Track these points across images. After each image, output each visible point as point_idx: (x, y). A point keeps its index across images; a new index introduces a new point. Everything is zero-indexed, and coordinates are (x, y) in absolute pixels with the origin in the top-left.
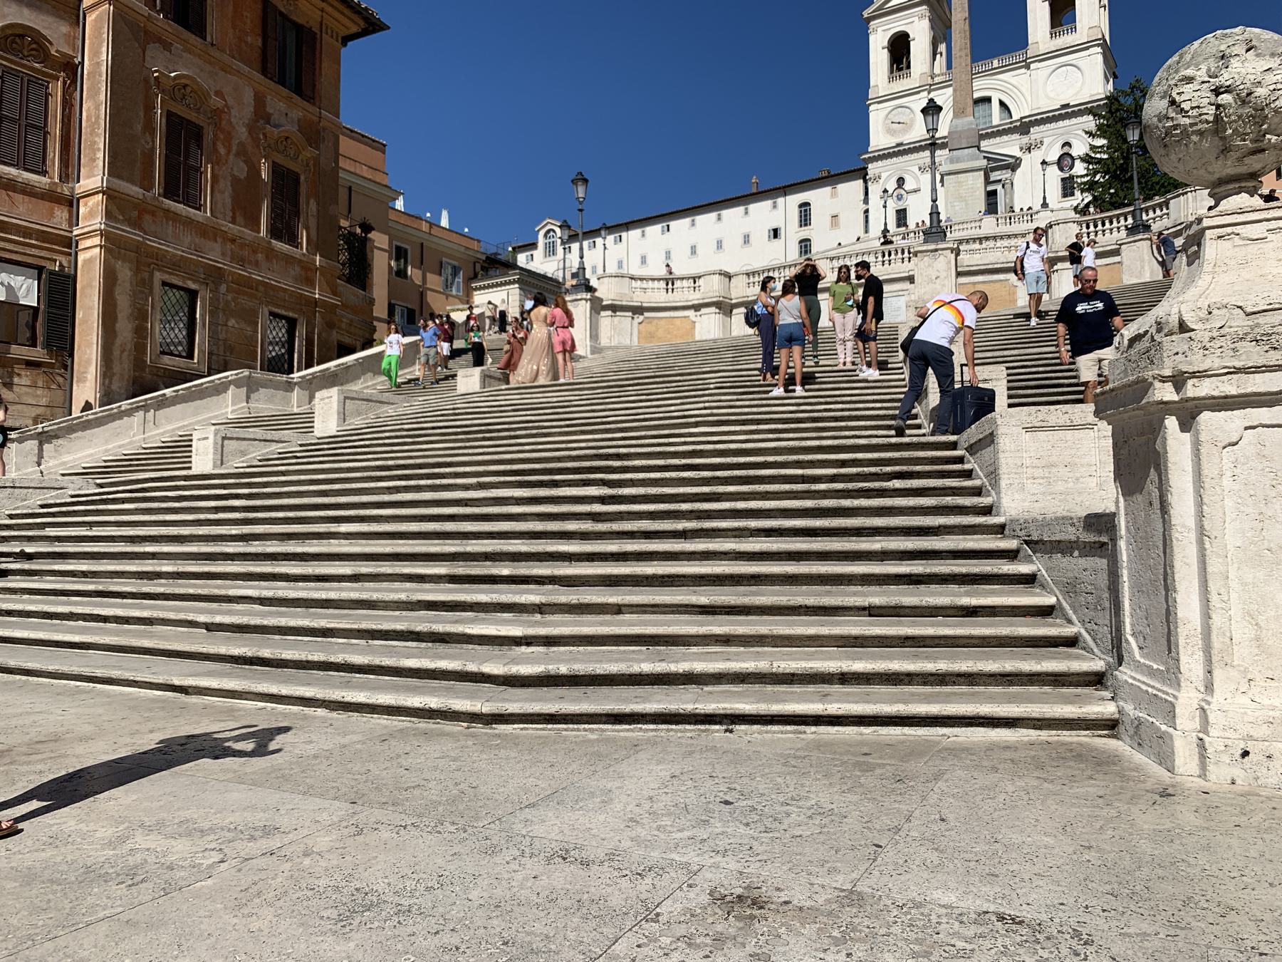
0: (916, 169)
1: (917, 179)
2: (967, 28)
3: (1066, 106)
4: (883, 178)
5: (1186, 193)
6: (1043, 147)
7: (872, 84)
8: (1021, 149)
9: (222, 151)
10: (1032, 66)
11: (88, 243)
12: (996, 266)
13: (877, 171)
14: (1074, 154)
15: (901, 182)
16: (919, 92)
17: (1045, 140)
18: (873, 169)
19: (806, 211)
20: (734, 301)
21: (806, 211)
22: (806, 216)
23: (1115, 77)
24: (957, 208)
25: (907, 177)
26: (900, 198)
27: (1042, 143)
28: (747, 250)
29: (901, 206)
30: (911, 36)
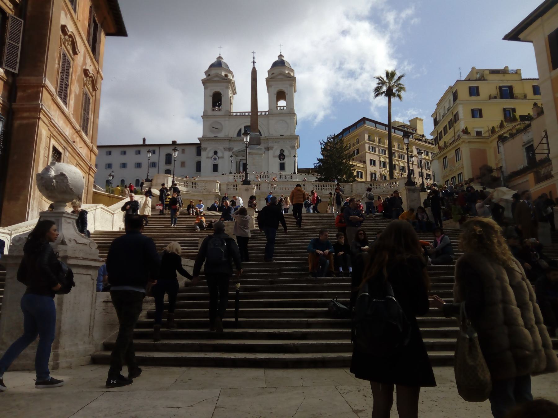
3: (283, 135)
4: (209, 149)
6: (274, 149)
9: (74, 77)
11: (26, 115)
15: (216, 153)
26: (215, 159)
29: (215, 162)
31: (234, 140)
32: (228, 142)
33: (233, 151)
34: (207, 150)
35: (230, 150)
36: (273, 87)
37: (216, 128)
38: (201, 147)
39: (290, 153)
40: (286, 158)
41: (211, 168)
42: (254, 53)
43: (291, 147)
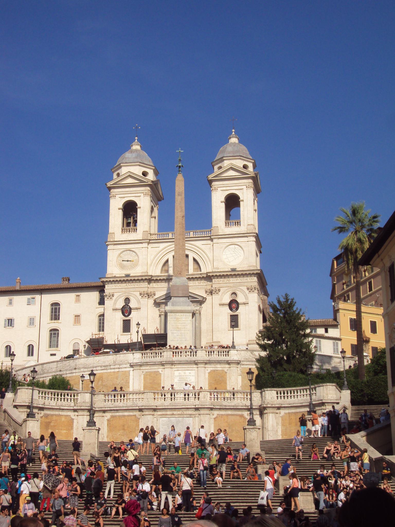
0: (138, 294)
1: (139, 302)
2: (184, 222)
4: (116, 295)
5: (323, 386)
6: (220, 293)
7: (111, 231)
8: (206, 292)
10: (215, 241)
12: (238, 407)
13: (111, 291)
14: (239, 301)
15: (127, 300)
16: (141, 243)
17: (221, 289)
18: (109, 289)
19: (56, 309)
20: (97, 409)
21: (56, 309)
22: (56, 312)
23: (260, 252)
24: (175, 334)
25: (132, 299)
27: (219, 290)
28: (9, 329)
30: (139, 205)
31: (157, 280)
32: (147, 283)
33: (156, 297)
34: (114, 298)
35: (149, 295)
36: (219, 189)
37: (128, 261)
38: (104, 291)
39: (246, 298)
40: (240, 307)
41: (119, 325)
42: (180, 152)
43: (248, 289)
